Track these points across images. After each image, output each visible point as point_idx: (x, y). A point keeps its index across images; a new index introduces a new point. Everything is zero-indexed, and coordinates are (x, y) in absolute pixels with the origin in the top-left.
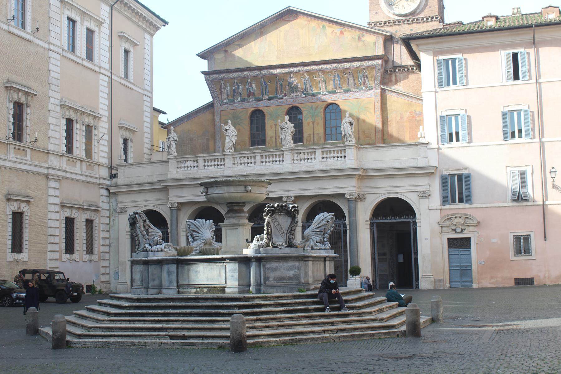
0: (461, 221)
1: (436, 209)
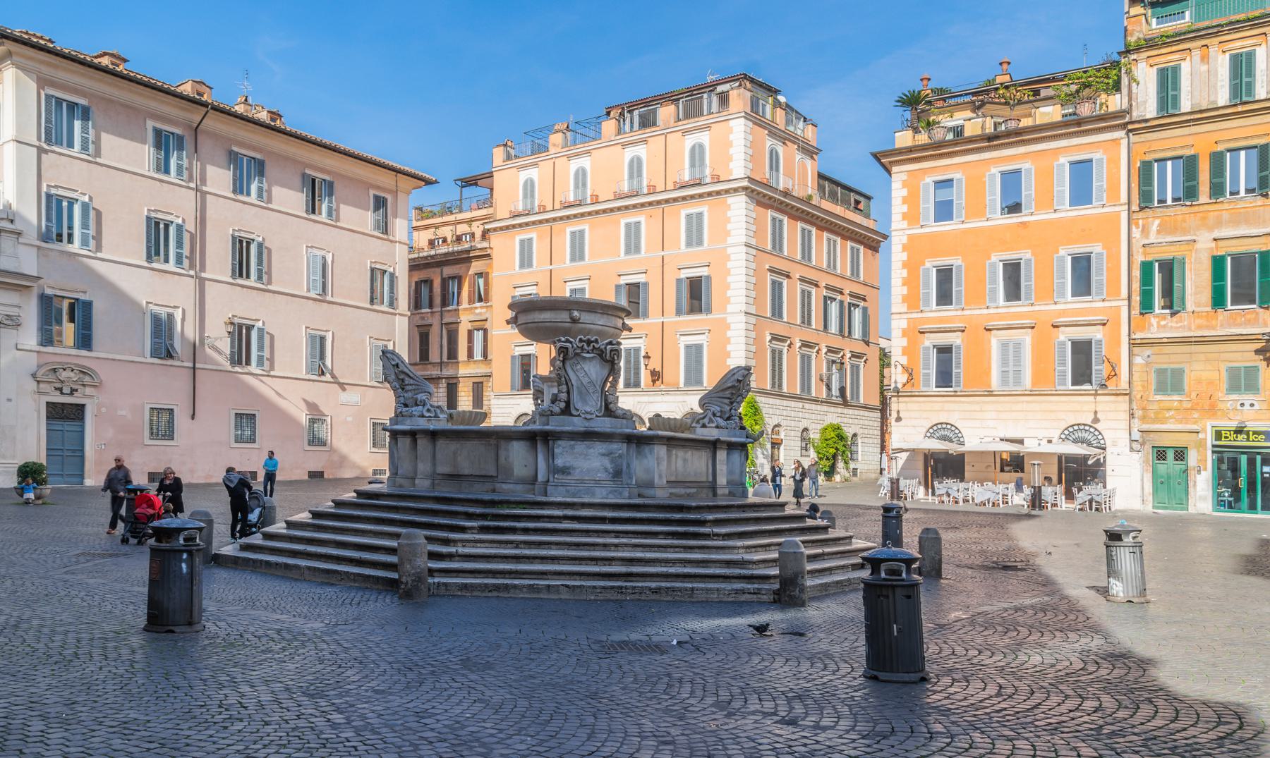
1: (31, 351)
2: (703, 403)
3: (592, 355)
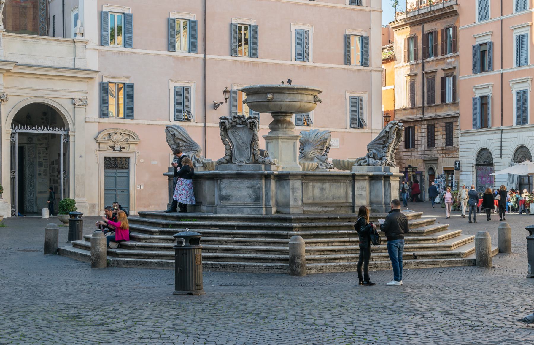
2: (368, 148)
3: (242, 126)
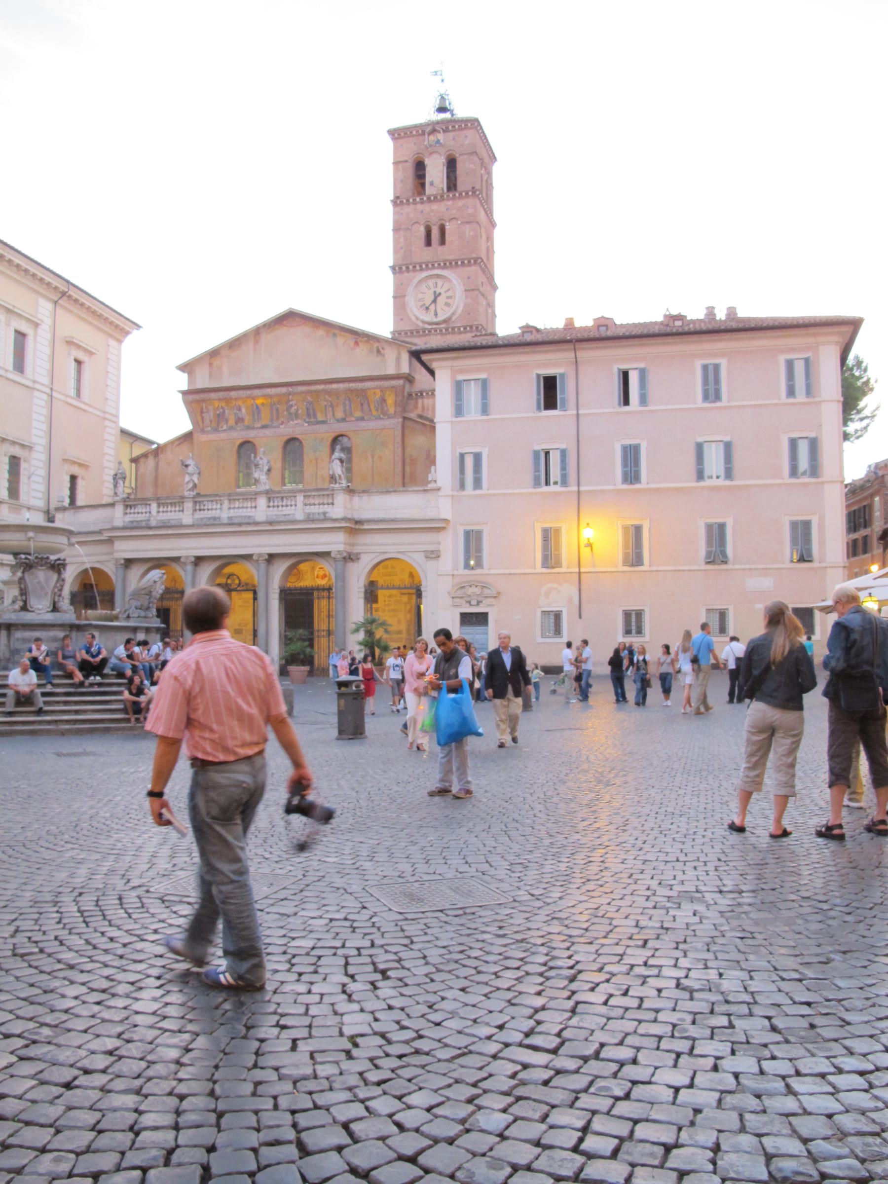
0: (477, 591)
